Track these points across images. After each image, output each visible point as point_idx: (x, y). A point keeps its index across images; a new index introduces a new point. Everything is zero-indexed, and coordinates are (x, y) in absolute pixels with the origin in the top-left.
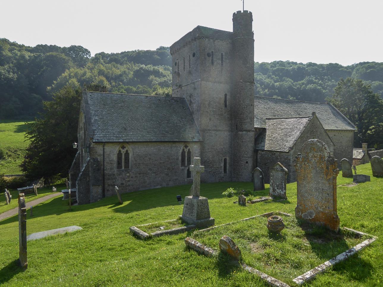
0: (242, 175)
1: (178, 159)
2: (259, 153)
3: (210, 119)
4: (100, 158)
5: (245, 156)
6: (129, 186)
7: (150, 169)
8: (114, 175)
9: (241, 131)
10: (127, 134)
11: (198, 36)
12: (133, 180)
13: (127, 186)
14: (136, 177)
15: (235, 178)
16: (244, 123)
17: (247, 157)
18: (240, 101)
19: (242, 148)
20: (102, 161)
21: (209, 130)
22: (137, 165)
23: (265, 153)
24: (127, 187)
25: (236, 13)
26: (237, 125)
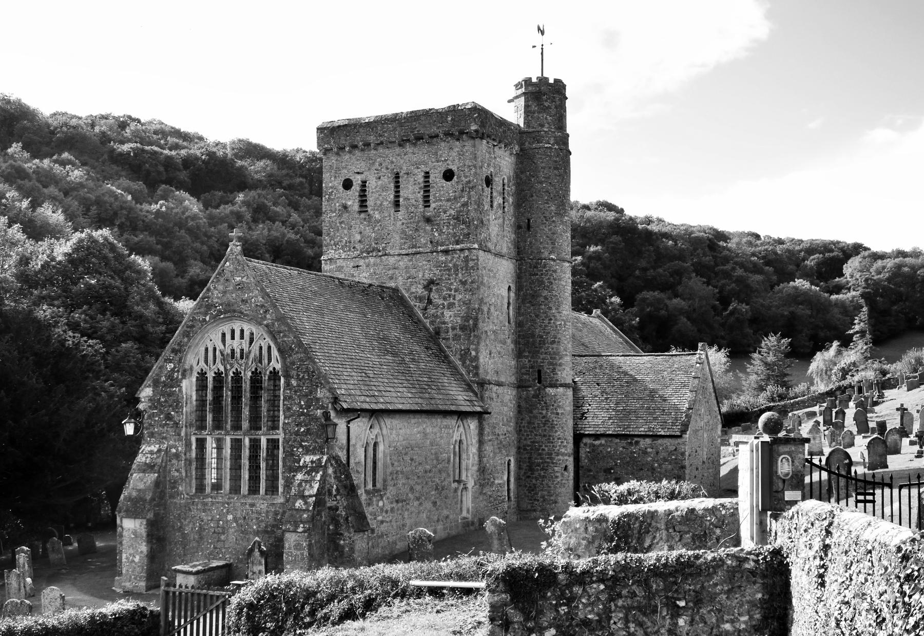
0: (556, 502)
1: (449, 461)
2: (585, 444)
4: (342, 455)
5: (563, 450)
9: (552, 386)
11: (476, 131)
12: (388, 520)
14: (392, 509)
15: (535, 510)
16: (560, 365)
17: (566, 455)
18: (550, 308)
19: (556, 431)
23: (603, 442)
26: (539, 372)
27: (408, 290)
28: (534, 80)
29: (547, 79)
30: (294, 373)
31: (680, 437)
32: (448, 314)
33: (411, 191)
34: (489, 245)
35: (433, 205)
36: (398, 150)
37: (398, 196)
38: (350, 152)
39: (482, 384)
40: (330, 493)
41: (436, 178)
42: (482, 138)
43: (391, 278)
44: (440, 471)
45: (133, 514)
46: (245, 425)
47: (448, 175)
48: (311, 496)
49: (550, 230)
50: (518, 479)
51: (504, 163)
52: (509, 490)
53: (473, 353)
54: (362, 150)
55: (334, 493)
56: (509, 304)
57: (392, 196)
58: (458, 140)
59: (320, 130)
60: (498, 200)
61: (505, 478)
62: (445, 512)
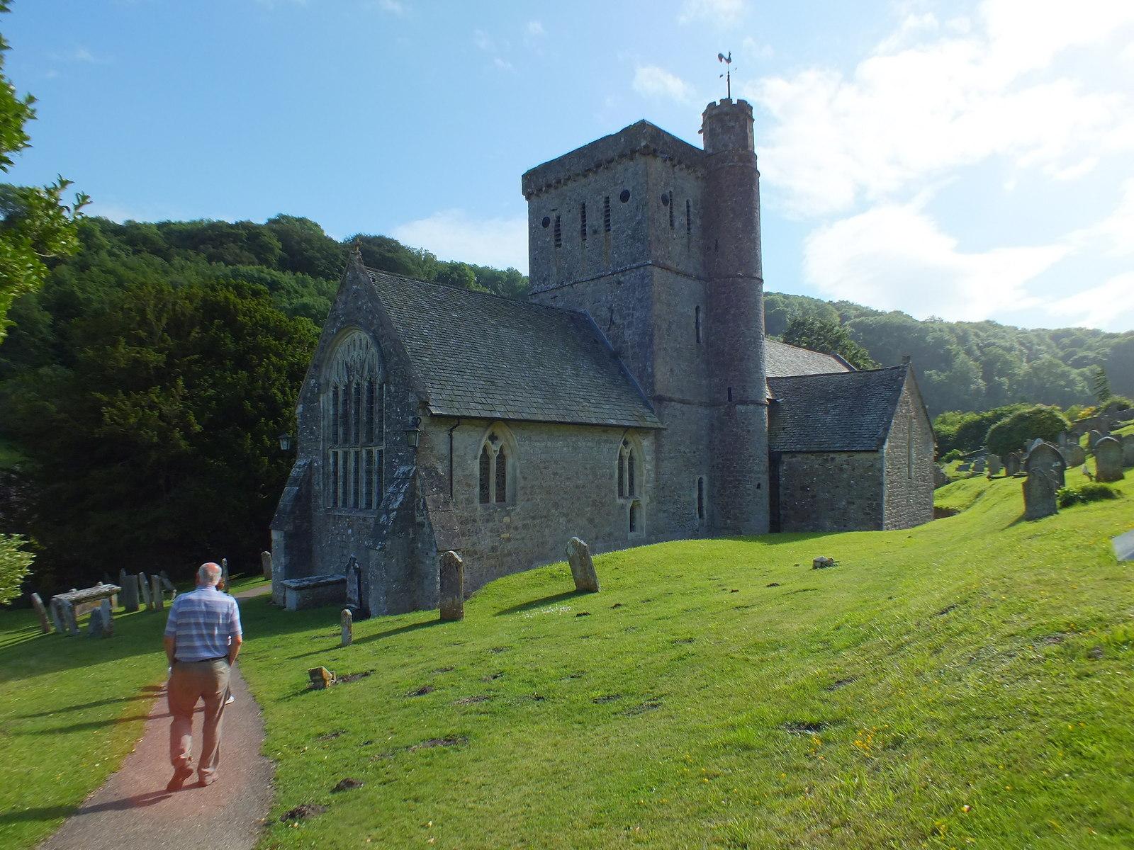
1: (611, 477)
6: (510, 554)
7: (556, 505)
8: (474, 521)
9: (744, 403)
10: (504, 397)
13: (505, 556)
14: (525, 526)
19: (747, 449)
20: (447, 477)
21: (671, 400)
22: (528, 492)
24: (505, 560)
25: (718, 103)
27: (594, 314)
28: (718, 103)
29: (729, 100)
30: (391, 378)
31: (877, 451)
32: (628, 332)
33: (595, 220)
34: (669, 263)
35: (613, 228)
36: (583, 181)
37: (585, 225)
38: (546, 192)
39: (660, 399)
40: (418, 507)
41: (615, 200)
42: (655, 156)
43: (581, 304)
45: (279, 528)
46: (363, 439)
47: (625, 196)
48: (393, 511)
49: (736, 247)
50: (711, 497)
51: (689, 187)
52: (700, 508)
53: (650, 370)
54: (556, 188)
55: (422, 508)
56: (697, 322)
57: (580, 227)
58: (632, 159)
59: (539, 183)
60: (680, 220)
61: (696, 495)
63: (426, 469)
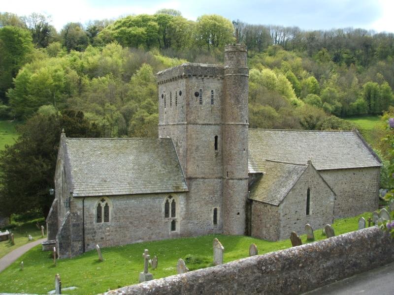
1: (160, 212)
3: (197, 166)
6: (109, 240)
7: (131, 223)
8: (94, 229)
11: (185, 75)
14: (116, 231)
20: (82, 215)
44: (153, 215)
50: (221, 216)
62: (158, 231)
63: (73, 213)
